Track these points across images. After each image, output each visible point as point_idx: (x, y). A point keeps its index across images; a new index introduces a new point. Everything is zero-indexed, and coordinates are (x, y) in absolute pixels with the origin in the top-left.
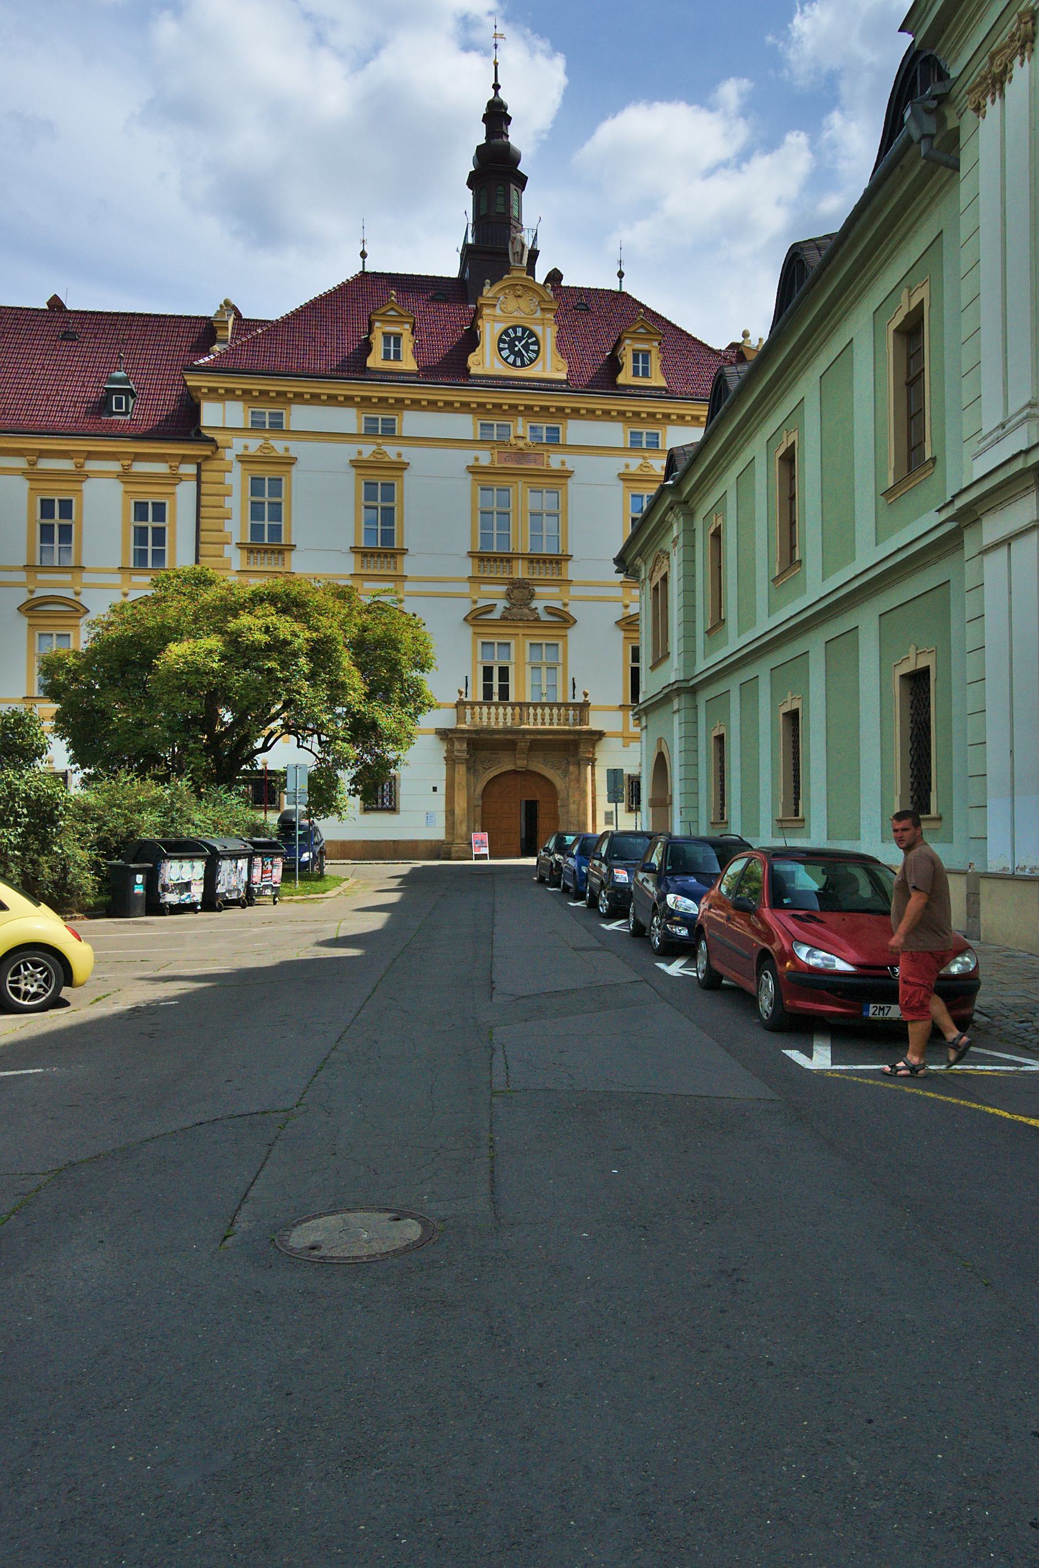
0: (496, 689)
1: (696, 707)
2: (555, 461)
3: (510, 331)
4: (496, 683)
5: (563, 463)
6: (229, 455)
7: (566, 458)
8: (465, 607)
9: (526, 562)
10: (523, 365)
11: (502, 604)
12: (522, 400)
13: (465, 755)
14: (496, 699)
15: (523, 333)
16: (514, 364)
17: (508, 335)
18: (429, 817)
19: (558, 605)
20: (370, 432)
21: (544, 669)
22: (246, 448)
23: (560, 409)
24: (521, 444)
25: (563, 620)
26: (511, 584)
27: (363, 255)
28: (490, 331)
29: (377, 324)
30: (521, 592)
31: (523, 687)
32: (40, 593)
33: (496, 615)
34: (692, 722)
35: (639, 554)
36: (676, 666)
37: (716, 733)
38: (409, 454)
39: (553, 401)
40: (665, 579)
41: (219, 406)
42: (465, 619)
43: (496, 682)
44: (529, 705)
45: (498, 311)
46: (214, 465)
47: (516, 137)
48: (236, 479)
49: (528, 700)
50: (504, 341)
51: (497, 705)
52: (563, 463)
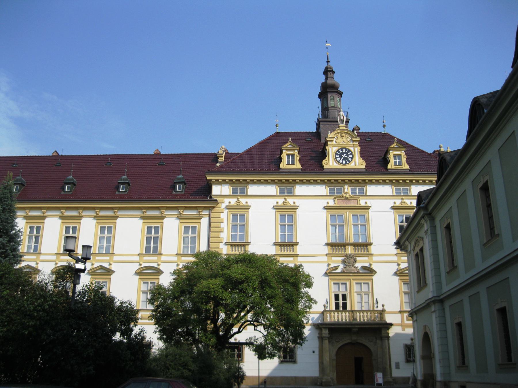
0: (341, 305)
1: (444, 309)
2: (362, 202)
3: (340, 150)
4: (341, 302)
5: (366, 203)
6: (223, 206)
7: (367, 201)
9: (352, 247)
10: (346, 163)
12: (347, 178)
13: (328, 335)
14: (341, 309)
15: (346, 151)
16: (342, 163)
17: (339, 152)
22: (230, 202)
23: (364, 181)
24: (347, 196)
25: (370, 271)
28: (331, 150)
29: (284, 151)
30: (349, 260)
31: (355, 303)
32: (144, 265)
33: (339, 270)
34: (442, 317)
35: (407, 239)
36: (431, 289)
37: (457, 321)
39: (360, 178)
40: (422, 250)
41: (219, 187)
42: (326, 273)
43: (341, 301)
44: (356, 311)
45: (334, 143)
46: (215, 210)
47: (337, 79)
48: (225, 215)
50: (338, 155)
51: (341, 312)
52: (366, 203)
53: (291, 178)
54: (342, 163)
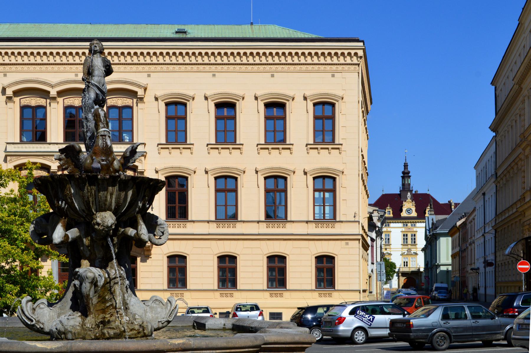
8: (400, 253)
25: (416, 254)
28: (404, 209)
30: (409, 250)
31: (410, 265)
38: (391, 230)
43: (406, 264)
47: (409, 169)
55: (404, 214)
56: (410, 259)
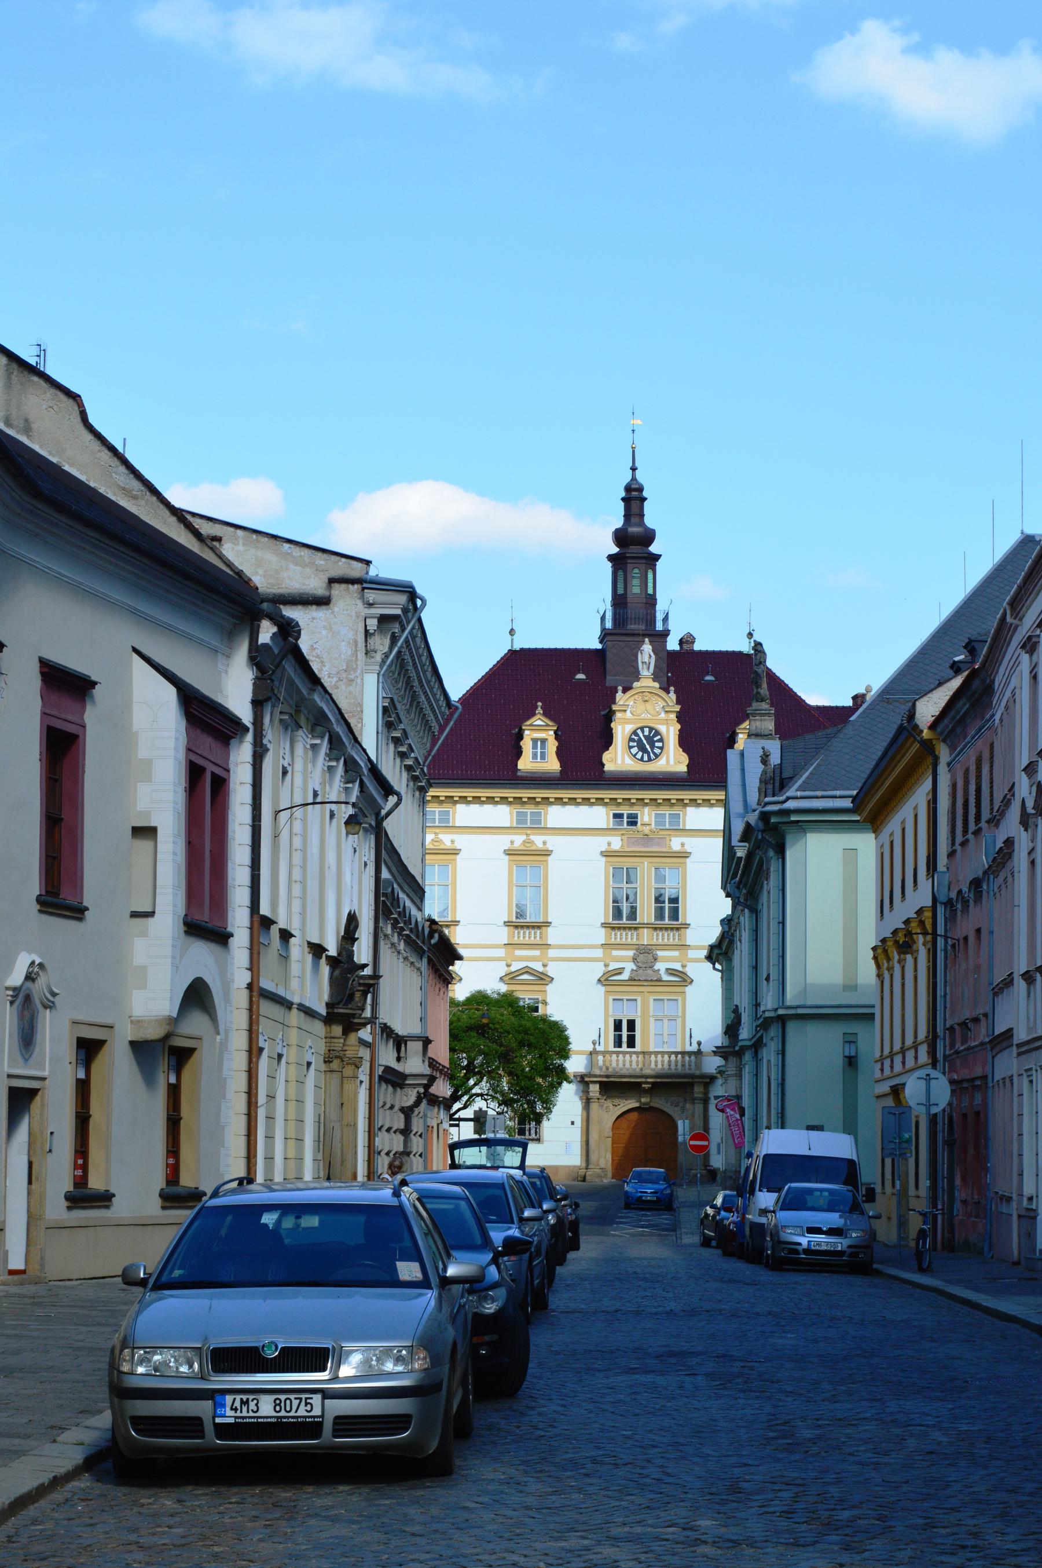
0: (625, 1039)
2: (675, 844)
3: (639, 731)
4: (625, 1033)
5: (683, 845)
8: (599, 970)
10: (650, 760)
11: (630, 966)
16: (642, 759)
18: (568, 1146)
19: (677, 966)
20: (520, 826)
21: (666, 1021)
25: (684, 979)
26: (637, 950)
27: (512, 632)
28: (621, 730)
30: (645, 956)
33: (625, 976)
39: (673, 795)
42: (599, 980)
43: (625, 1032)
44: (651, 1053)
45: (628, 714)
49: (652, 1050)
53: (539, 794)
54: (642, 759)
55: (618, 759)
56: (642, 1007)
